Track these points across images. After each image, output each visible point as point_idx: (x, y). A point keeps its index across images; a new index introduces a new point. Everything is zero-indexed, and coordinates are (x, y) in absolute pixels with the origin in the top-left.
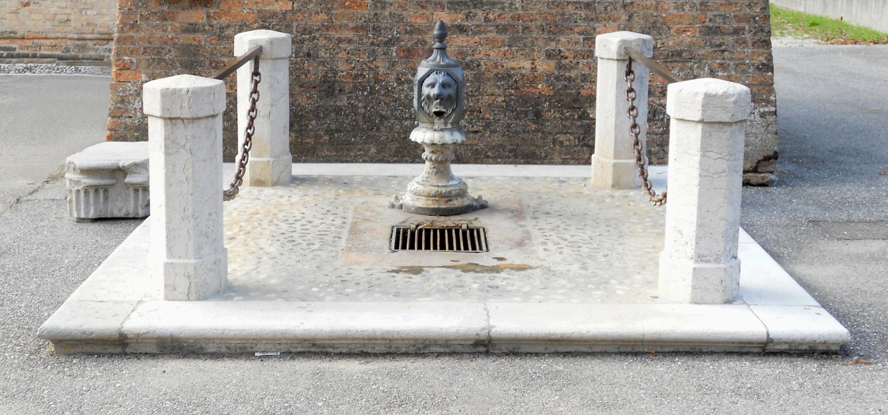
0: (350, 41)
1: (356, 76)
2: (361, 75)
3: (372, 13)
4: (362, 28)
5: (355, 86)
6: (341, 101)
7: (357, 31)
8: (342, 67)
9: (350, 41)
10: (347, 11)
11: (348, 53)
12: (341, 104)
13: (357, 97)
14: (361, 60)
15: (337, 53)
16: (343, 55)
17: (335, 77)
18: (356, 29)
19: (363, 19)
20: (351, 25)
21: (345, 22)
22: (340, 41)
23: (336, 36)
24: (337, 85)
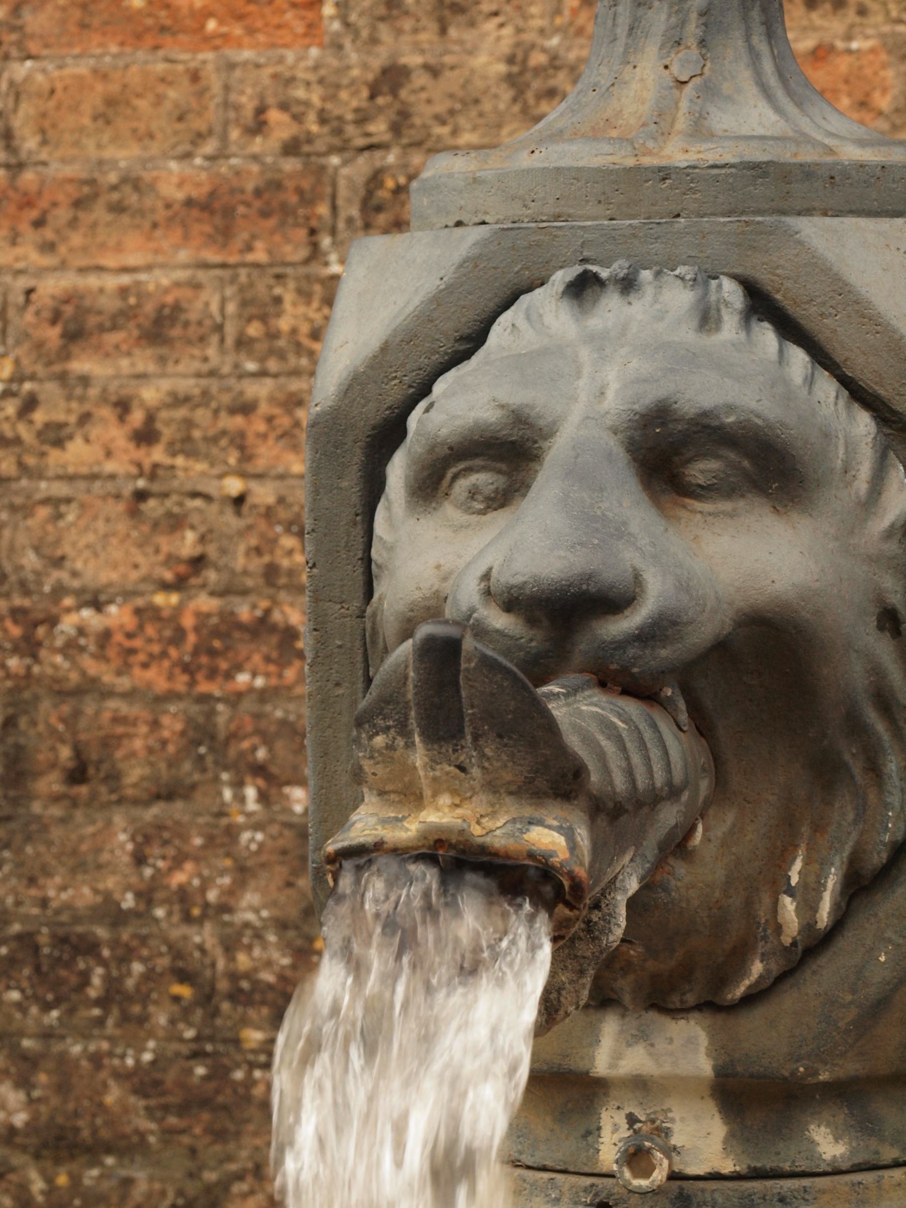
0: (161, 328)
1: (221, 641)
2: (262, 626)
3: (360, 64)
4: (276, 202)
5: (200, 733)
6: (81, 865)
7: (225, 234)
8: (104, 553)
9: (161, 328)
10: (145, 64)
11: (146, 436)
12: (84, 895)
13: (223, 837)
14: (264, 494)
15: (55, 436)
16: (101, 449)
17: (29, 647)
18: (214, 211)
19: (281, 126)
20: (176, 178)
21: (124, 156)
22: (76, 326)
23: (51, 287)
24: (49, 713)
